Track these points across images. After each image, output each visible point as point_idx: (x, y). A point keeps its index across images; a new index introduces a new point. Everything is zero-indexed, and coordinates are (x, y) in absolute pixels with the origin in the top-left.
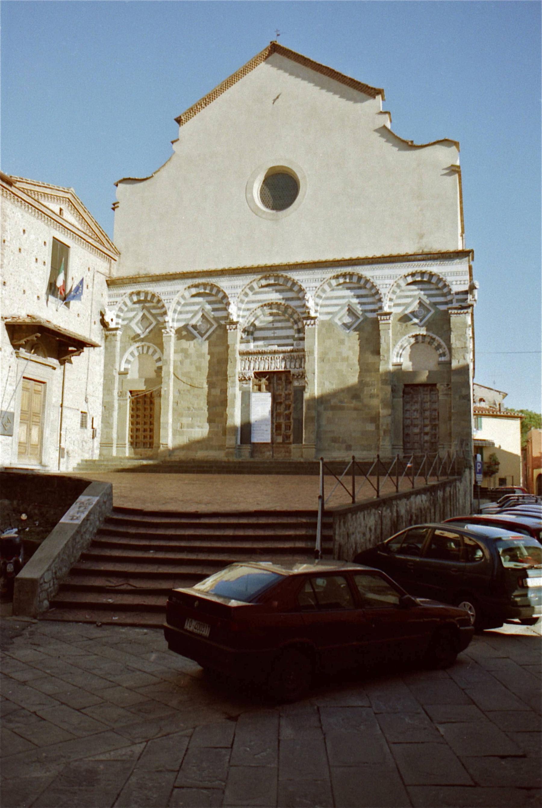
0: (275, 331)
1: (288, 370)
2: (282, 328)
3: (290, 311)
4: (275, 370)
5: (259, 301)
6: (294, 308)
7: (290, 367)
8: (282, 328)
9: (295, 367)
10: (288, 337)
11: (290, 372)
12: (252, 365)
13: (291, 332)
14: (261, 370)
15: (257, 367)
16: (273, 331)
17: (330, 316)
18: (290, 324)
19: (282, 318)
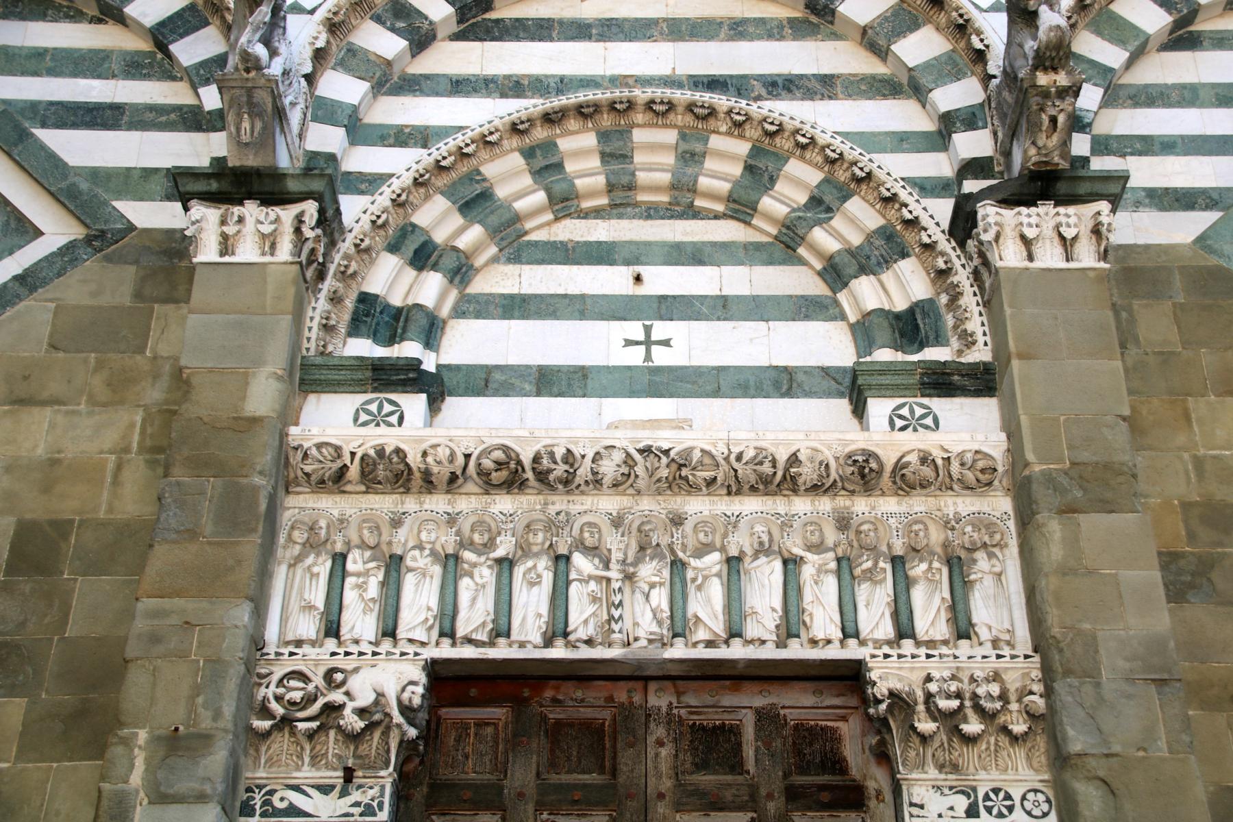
0: (661, 329)
1: (833, 653)
2: (722, 308)
3: (798, 180)
4: (679, 651)
5: (514, 87)
6: (851, 152)
7: (850, 632)
8: (722, 308)
9: (904, 630)
10: (785, 382)
11: (850, 676)
12: (419, 600)
13: (829, 345)
14: (527, 639)
15: (474, 613)
16: (635, 329)
17: (1201, 221)
18: (798, 280)
19: (729, 231)
